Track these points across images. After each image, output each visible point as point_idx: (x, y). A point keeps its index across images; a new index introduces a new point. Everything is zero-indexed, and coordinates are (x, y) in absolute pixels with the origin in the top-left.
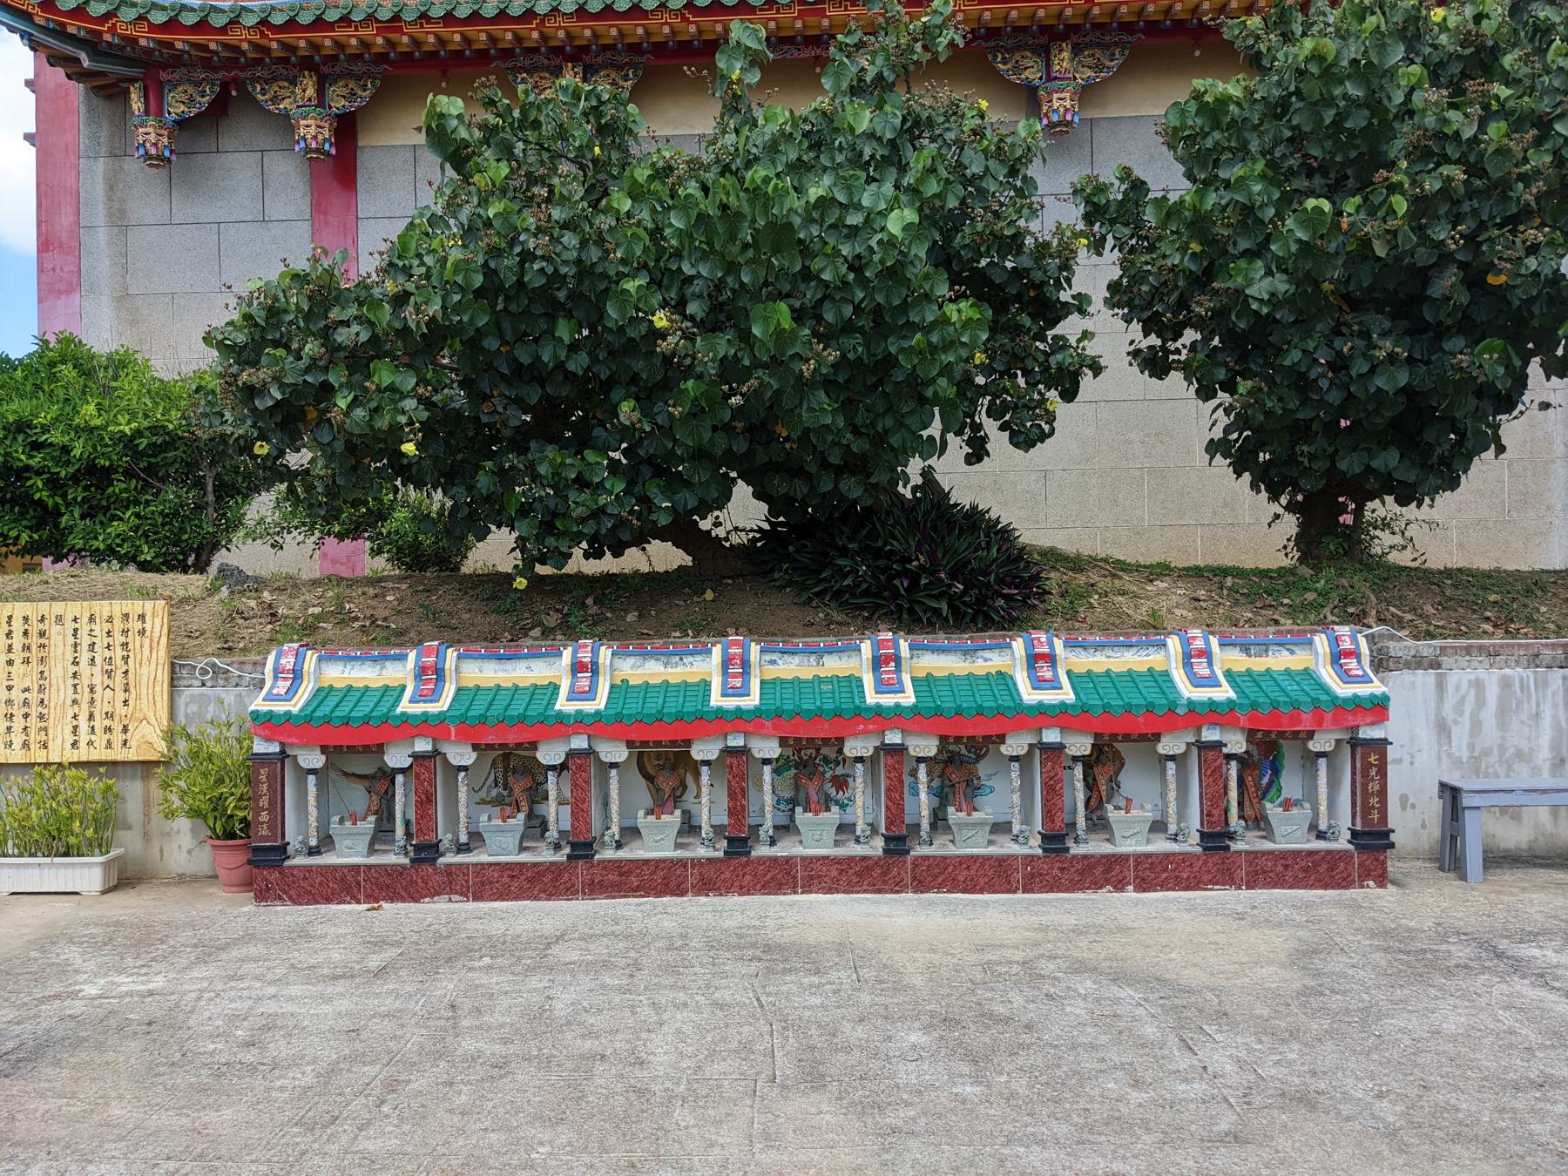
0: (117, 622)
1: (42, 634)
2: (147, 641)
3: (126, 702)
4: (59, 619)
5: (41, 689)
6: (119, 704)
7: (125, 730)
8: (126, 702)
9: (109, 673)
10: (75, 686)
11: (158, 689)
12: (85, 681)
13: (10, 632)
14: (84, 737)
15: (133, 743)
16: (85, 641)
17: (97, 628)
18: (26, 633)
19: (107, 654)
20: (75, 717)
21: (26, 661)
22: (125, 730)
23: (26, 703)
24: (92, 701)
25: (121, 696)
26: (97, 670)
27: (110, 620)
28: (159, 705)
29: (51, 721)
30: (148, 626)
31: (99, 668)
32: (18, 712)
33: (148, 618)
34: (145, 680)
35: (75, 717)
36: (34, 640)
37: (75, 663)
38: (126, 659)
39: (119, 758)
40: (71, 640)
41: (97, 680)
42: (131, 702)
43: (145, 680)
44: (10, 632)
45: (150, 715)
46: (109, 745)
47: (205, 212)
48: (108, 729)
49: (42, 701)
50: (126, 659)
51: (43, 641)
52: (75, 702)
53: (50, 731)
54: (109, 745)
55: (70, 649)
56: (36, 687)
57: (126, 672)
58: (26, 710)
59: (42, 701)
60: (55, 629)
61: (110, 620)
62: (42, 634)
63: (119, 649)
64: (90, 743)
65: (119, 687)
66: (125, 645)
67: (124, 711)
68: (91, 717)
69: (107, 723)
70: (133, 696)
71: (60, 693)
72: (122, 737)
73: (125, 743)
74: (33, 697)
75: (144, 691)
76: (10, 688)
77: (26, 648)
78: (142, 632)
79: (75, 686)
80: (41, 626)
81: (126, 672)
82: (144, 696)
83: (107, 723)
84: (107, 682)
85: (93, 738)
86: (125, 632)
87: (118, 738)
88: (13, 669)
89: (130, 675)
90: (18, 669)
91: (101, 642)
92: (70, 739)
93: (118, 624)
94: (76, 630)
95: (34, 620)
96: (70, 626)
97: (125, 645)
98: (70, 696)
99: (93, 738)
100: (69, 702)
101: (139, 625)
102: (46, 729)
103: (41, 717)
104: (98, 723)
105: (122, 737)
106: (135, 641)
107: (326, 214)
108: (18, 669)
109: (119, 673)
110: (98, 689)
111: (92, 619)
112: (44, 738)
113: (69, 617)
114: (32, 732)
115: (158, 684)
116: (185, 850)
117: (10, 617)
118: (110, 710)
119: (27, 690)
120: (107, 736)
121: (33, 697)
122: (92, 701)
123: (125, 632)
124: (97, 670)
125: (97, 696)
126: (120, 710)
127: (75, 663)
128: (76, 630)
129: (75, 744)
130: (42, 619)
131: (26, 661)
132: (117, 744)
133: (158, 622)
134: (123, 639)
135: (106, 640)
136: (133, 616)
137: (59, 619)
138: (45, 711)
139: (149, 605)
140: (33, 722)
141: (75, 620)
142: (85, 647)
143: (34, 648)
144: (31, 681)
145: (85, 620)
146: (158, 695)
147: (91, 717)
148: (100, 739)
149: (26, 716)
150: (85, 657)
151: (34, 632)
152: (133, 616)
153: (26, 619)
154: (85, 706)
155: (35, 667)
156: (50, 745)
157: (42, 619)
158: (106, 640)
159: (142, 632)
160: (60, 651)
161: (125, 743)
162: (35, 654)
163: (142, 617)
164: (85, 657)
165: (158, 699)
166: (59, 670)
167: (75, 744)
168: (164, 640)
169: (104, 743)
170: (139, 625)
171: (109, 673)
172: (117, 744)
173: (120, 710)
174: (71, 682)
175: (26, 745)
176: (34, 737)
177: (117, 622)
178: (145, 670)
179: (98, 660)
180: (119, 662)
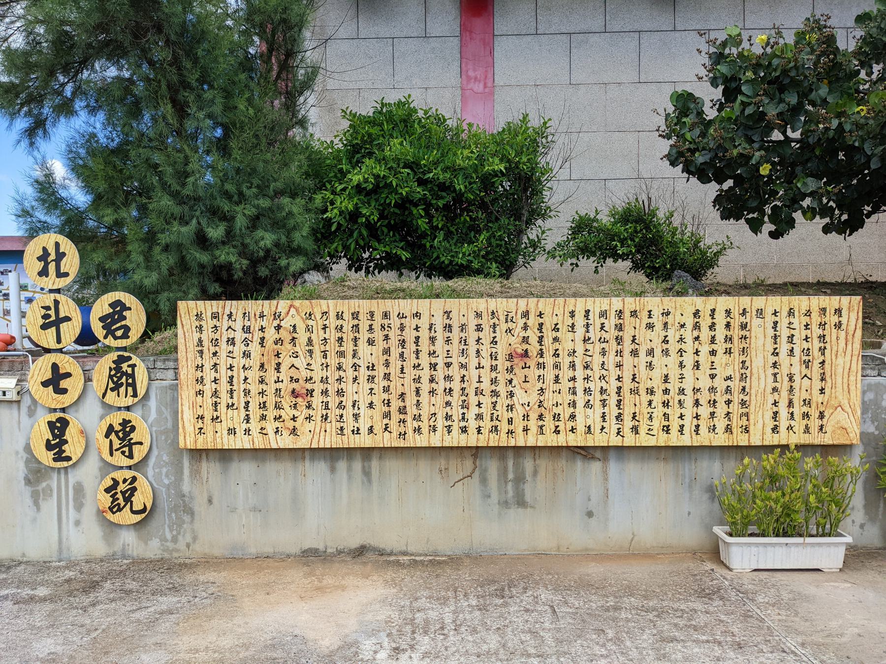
0: (815, 316)
1: (744, 326)
2: (842, 334)
3: (822, 391)
4: (760, 313)
5: (743, 377)
6: (816, 392)
7: (822, 416)
8: (822, 391)
9: (807, 364)
10: (775, 375)
11: (852, 378)
12: (784, 370)
13: (713, 324)
14: (784, 423)
15: (828, 428)
16: (784, 333)
17: (795, 321)
18: (728, 325)
19: (805, 345)
20: (775, 403)
21: (728, 352)
22: (822, 416)
23: (728, 390)
24: (791, 389)
25: (817, 385)
26: (796, 360)
27: (808, 313)
28: (853, 393)
29: (752, 407)
30: (844, 320)
31: (797, 358)
32: (721, 399)
33: (844, 313)
34: (840, 370)
35: (775, 403)
36: (736, 333)
37: (775, 353)
38: (822, 350)
39: (817, 442)
40: (771, 332)
41: (796, 370)
42: (827, 391)
43: (840, 370)
44: (713, 324)
45: (845, 403)
46: (807, 430)
47: (383, 30)
48: (806, 416)
49: (744, 389)
50: (822, 350)
51: (744, 333)
52: (775, 390)
53: (752, 417)
54: (807, 430)
55: (770, 341)
56: (738, 376)
57: (823, 363)
58: (728, 396)
59: (744, 389)
60: (755, 323)
61: (808, 313)
62: (744, 326)
63: (816, 341)
64: (790, 428)
65: (816, 377)
66: (822, 338)
67: (820, 398)
68: (790, 404)
69: (805, 409)
70: (829, 384)
71: (761, 381)
72: (818, 422)
73: (821, 427)
74: (735, 385)
75: (839, 381)
76: (713, 377)
77: (728, 339)
78: (838, 326)
79: (775, 375)
80: (742, 319)
81: (823, 363)
82: (839, 384)
83: (805, 409)
84: (805, 371)
85: (793, 423)
86: (822, 325)
87: (815, 423)
88: (716, 359)
89: (827, 366)
90: (721, 359)
91: (800, 334)
92: (771, 424)
93: (816, 318)
94: (776, 323)
95: (735, 313)
96: (770, 319)
97: (822, 338)
98: (771, 384)
99: (793, 423)
100: (769, 390)
101: (835, 319)
102: (747, 415)
103: (743, 403)
104: (798, 410)
105: (818, 422)
106: (831, 333)
107: (471, 32)
108: (721, 359)
109: (816, 362)
110: (797, 378)
111: (791, 313)
112: (745, 423)
113: (769, 311)
114: (735, 417)
115: (853, 374)
116: (858, 523)
117: (713, 311)
118: (808, 397)
119: (729, 378)
120: (805, 422)
121: (735, 385)
122: (791, 389)
123: (822, 325)
124: (796, 360)
125: (796, 385)
126: (817, 398)
127: (775, 353)
128: (776, 323)
129: (775, 429)
130: (744, 312)
131: (728, 352)
132: (814, 429)
133: (853, 316)
134: (820, 332)
135: (804, 333)
136: (830, 311)
137: (760, 313)
138: (746, 398)
139: (845, 300)
140: (735, 408)
141: (775, 313)
142: (784, 339)
143: (736, 339)
144: (734, 370)
145: (785, 313)
146: (852, 383)
147: (790, 404)
148: (799, 424)
149: (728, 402)
150: (784, 348)
151: (736, 324)
152: (830, 311)
153: (728, 312)
154: (784, 394)
155: (737, 357)
156: (751, 429)
157: (744, 312)
158: (804, 333)
159: (838, 326)
160: (760, 342)
161: (821, 427)
162: (736, 345)
163: (838, 312)
164: (784, 348)
165: (852, 388)
166: (759, 360)
167: (775, 429)
168: (859, 333)
169: (803, 428)
170: (835, 319)
171: (807, 364)
172: (814, 429)
173: (817, 398)
174: (772, 371)
175: (728, 429)
176: (735, 422)
177: (815, 316)
178: (840, 360)
179: (797, 351)
180: (816, 353)
